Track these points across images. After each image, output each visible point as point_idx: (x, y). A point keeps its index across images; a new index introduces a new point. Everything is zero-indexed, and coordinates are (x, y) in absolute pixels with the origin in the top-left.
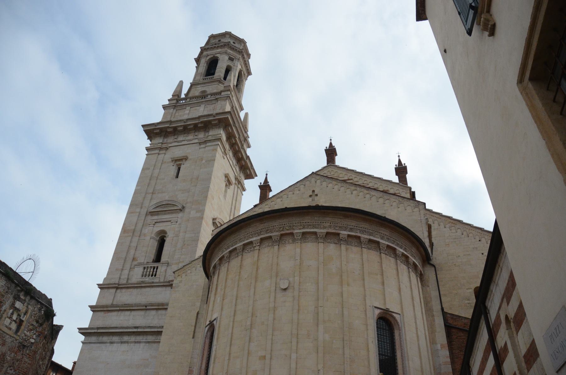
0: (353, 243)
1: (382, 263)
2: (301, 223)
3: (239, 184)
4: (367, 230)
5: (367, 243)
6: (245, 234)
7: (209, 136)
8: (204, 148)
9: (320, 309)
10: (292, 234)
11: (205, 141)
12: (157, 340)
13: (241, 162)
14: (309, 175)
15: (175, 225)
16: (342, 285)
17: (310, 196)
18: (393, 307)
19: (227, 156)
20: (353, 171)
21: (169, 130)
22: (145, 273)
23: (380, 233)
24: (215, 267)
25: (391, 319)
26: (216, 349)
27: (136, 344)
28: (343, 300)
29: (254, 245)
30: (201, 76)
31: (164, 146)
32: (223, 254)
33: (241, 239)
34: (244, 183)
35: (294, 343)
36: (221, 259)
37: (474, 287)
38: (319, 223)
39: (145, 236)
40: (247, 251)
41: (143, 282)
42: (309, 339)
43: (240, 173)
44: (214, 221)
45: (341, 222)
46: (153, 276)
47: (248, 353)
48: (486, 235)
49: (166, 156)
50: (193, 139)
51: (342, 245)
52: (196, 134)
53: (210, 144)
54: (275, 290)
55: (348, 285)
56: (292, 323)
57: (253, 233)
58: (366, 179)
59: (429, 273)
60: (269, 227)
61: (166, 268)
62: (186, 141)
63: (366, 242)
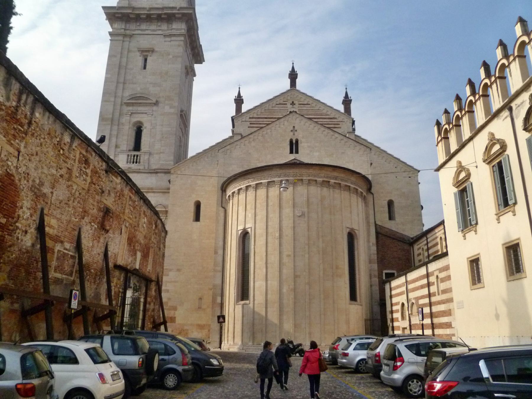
8: (169, 41)
17: (292, 131)
18: (355, 227)
20: (311, 97)
22: (129, 160)
31: (128, 32)
44: (182, 113)
49: (131, 44)
50: (157, 30)
52: (159, 24)
55: (334, 215)
59: (370, 198)
62: (149, 31)
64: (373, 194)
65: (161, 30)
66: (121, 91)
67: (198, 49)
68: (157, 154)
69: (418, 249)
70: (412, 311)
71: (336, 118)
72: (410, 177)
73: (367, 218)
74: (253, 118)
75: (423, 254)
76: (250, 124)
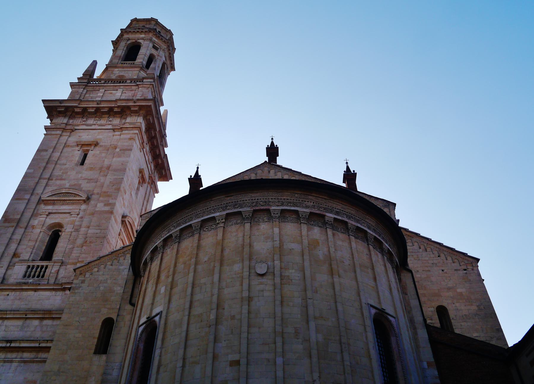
0: (340, 229)
2: (278, 199)
3: (152, 184)
4: (353, 217)
5: (354, 230)
6: (205, 208)
7: (126, 123)
8: (119, 135)
9: (310, 301)
10: (268, 211)
11: (121, 128)
12: (37, 358)
14: (262, 164)
15: (75, 218)
19: (144, 149)
21: (77, 110)
23: (366, 221)
24: (155, 250)
26: (161, 353)
27: (6, 364)
29: (217, 222)
30: (119, 60)
31: (69, 127)
32: (171, 233)
33: (197, 215)
34: (158, 183)
35: (279, 344)
36: (166, 241)
37: (437, 306)
38: (300, 201)
39: (33, 228)
40: (206, 229)
41: (25, 283)
42: (298, 339)
43: (154, 173)
44: (124, 219)
45: (325, 202)
46: (40, 278)
48: (445, 251)
49: (70, 139)
51: (328, 229)
53: (126, 132)
54: (249, 276)
56: (275, 318)
57: (216, 207)
60: (238, 201)
61: (58, 269)
63: (353, 229)
64: (411, 271)
65: (111, 124)
66: (43, 188)
67: (162, 159)
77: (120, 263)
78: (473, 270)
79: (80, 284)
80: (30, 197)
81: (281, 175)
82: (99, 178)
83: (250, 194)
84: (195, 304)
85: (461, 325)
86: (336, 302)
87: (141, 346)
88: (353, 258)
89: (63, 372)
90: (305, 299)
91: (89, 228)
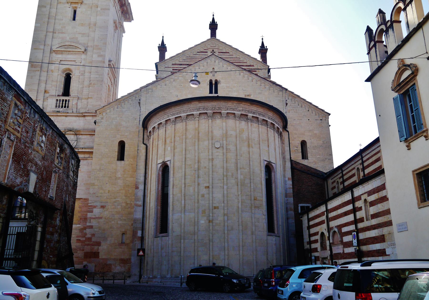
1: (268, 133)
4: (262, 113)
9: (238, 161)
10: (220, 113)
13: (123, 7)
16: (249, 147)
18: (273, 160)
25: (271, 167)
28: (249, 156)
35: (225, 180)
38: (236, 107)
44: (110, 63)
47: (198, 184)
58: (239, 54)
59: (285, 134)
61: (77, 102)
64: (288, 132)
66: (51, 40)
67: (126, 7)
68: (85, 99)
69: (333, 183)
70: (333, 240)
71: (253, 66)
72: (321, 120)
73: (283, 153)
74: (175, 64)
75: (338, 188)
76: (173, 70)
77: (123, 107)
78: (325, 120)
79: (101, 120)
80: (44, 47)
81: (222, 64)
82: (90, 33)
83: (212, 103)
84: (187, 159)
85: (312, 152)
86: (250, 161)
87: (161, 173)
88: (259, 137)
89: (102, 170)
90: (237, 160)
91: (91, 73)
